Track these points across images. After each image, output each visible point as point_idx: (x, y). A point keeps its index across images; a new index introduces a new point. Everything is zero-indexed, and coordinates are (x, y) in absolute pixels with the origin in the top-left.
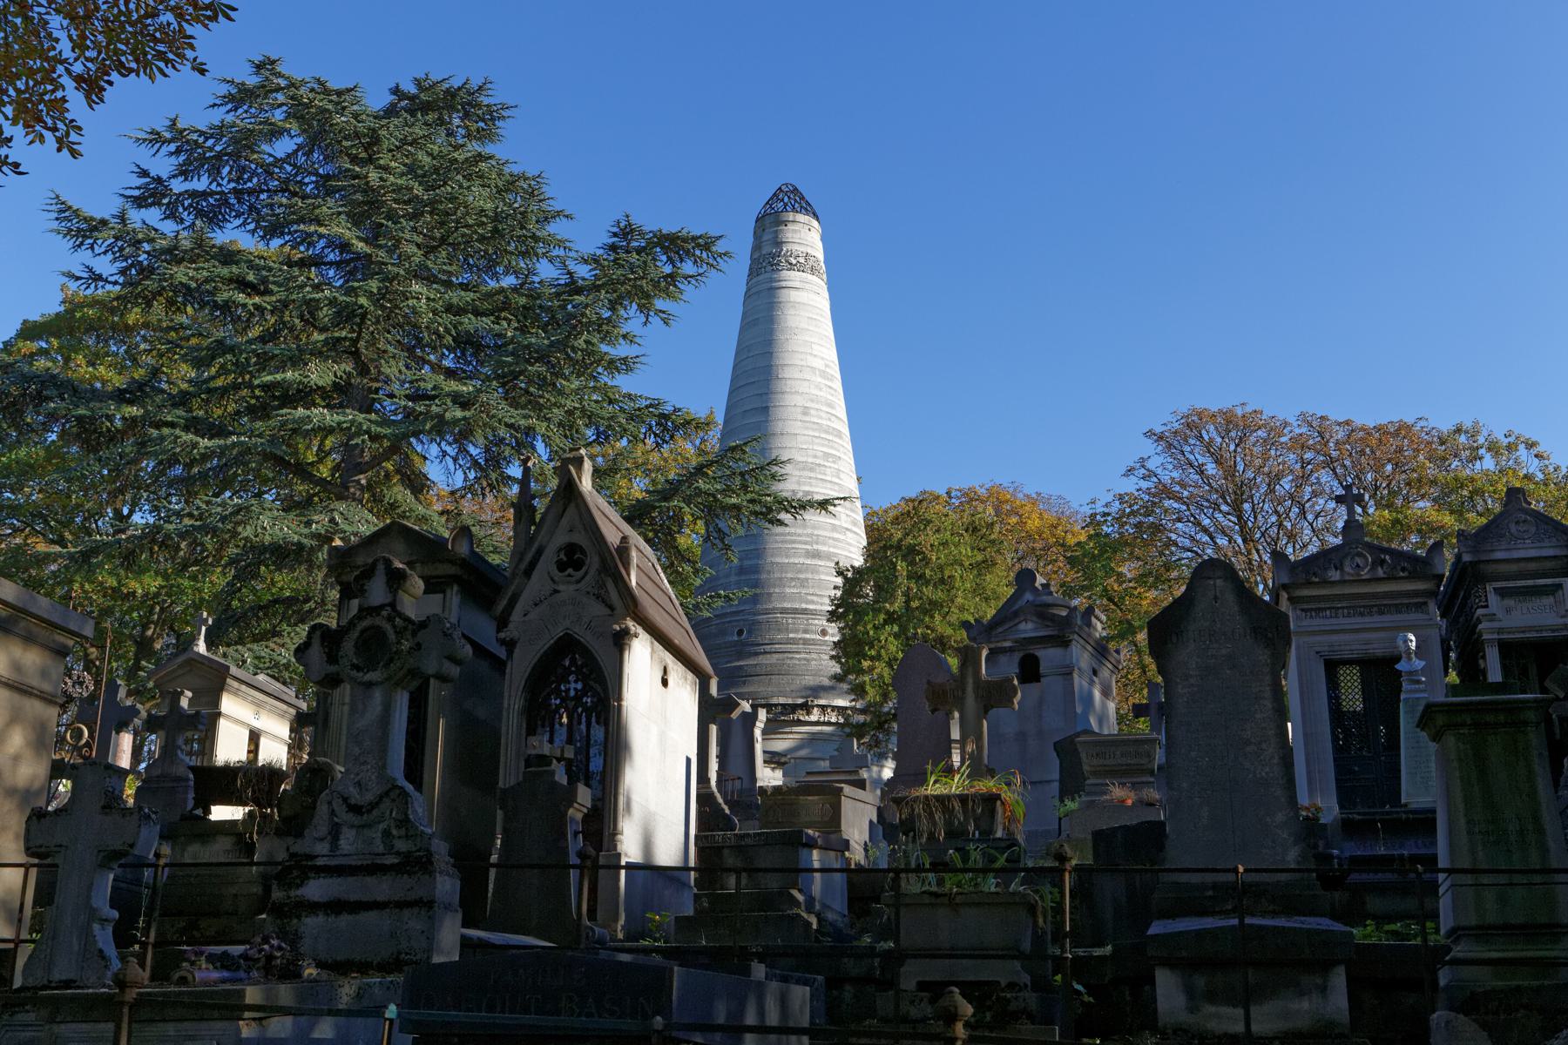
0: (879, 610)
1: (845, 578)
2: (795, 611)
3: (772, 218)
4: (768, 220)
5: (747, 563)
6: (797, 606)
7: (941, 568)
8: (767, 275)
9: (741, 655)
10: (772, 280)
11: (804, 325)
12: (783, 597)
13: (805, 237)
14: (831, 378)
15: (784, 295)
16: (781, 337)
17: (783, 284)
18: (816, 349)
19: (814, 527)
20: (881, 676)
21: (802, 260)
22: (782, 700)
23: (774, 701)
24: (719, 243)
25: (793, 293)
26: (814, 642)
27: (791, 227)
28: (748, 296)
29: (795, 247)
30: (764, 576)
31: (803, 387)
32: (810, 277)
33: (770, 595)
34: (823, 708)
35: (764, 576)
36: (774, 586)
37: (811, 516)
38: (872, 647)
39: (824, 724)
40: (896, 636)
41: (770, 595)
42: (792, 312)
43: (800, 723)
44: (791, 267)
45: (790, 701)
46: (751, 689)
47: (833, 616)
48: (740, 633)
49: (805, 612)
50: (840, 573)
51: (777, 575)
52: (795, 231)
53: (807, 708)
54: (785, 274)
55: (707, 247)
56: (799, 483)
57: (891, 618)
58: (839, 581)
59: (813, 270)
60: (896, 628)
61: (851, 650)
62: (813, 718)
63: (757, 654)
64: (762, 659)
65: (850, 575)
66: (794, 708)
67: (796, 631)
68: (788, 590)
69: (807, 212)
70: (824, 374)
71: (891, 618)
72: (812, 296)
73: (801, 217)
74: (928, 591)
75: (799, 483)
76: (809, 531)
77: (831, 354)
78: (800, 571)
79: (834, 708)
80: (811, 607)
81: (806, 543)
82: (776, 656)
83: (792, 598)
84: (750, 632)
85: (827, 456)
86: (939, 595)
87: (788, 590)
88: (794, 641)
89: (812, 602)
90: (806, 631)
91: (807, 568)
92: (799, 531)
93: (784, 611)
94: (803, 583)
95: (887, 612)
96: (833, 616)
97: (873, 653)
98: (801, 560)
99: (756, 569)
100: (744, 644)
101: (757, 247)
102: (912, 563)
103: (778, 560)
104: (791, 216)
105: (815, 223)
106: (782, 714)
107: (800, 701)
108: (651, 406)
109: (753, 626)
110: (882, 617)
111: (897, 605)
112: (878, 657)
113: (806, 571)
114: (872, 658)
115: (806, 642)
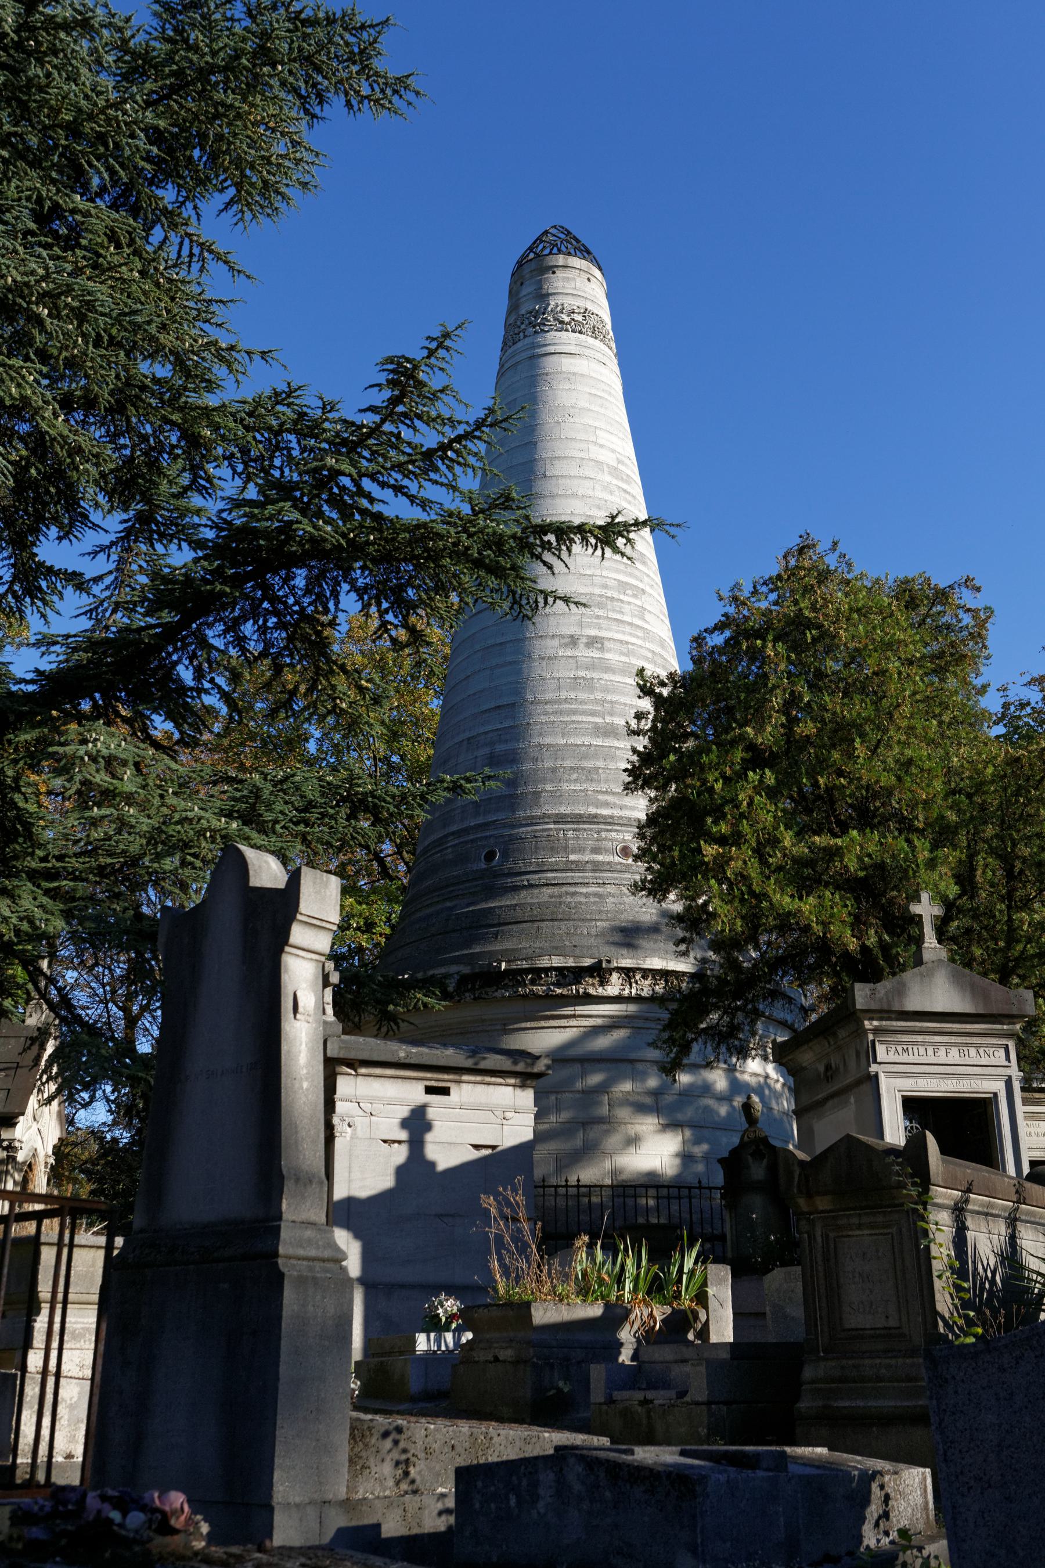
0: (733, 743)
1: (659, 702)
2: (578, 819)
3: (533, 265)
4: (527, 269)
5: (500, 748)
6: (580, 810)
7: (856, 656)
8: (527, 341)
9: (492, 892)
10: (535, 346)
11: (583, 403)
12: (558, 797)
13: (582, 288)
14: (628, 480)
15: (550, 363)
16: (548, 419)
17: (551, 349)
18: (603, 437)
19: (606, 690)
20: (744, 877)
21: (579, 318)
22: (557, 961)
23: (544, 962)
24: (386, 42)
25: (565, 361)
26: (610, 867)
27: (560, 273)
28: (501, 374)
29: (569, 302)
30: (527, 766)
31: (584, 488)
32: (591, 341)
33: (537, 795)
34: (628, 973)
35: (527, 766)
36: (544, 781)
37: (582, 556)
38: (720, 816)
39: (629, 999)
40: (773, 794)
41: (537, 795)
42: (565, 385)
43: (589, 999)
44: (562, 326)
45: (571, 963)
46: (507, 945)
47: (638, 777)
48: (490, 856)
49: (594, 819)
50: (646, 690)
51: (548, 764)
52: (568, 279)
53: (599, 972)
54: (553, 336)
55: (362, 58)
56: (581, 625)
57: (757, 758)
58: (646, 704)
59: (595, 332)
60: (770, 778)
61: (674, 845)
62: (612, 990)
63: (516, 889)
64: (524, 897)
65: (665, 692)
66: (578, 974)
67: (581, 850)
68: (565, 786)
69: (584, 258)
70: (614, 471)
71: (757, 758)
72: (594, 365)
73: (575, 262)
74: (833, 702)
75: (581, 625)
76: (599, 696)
77: (627, 448)
78: (585, 757)
79: (646, 973)
80: (605, 812)
81: (593, 714)
82: (549, 891)
83: (573, 798)
84: (505, 855)
85: (623, 586)
86: (859, 708)
87: (565, 786)
88: (578, 866)
89: (606, 805)
90: (596, 850)
91: (594, 752)
92: (582, 696)
93: (560, 819)
94: (591, 775)
95: (751, 747)
96: (638, 777)
97: (724, 828)
98: (587, 740)
99: (513, 758)
100: (497, 875)
101: (514, 306)
102: (797, 647)
103: (549, 740)
104: (561, 260)
105: (597, 273)
106: (558, 985)
107: (587, 962)
108: (277, 397)
109: (510, 845)
110: (739, 755)
111: (767, 735)
112: (736, 839)
113: (596, 756)
114: (721, 840)
115: (596, 867)
